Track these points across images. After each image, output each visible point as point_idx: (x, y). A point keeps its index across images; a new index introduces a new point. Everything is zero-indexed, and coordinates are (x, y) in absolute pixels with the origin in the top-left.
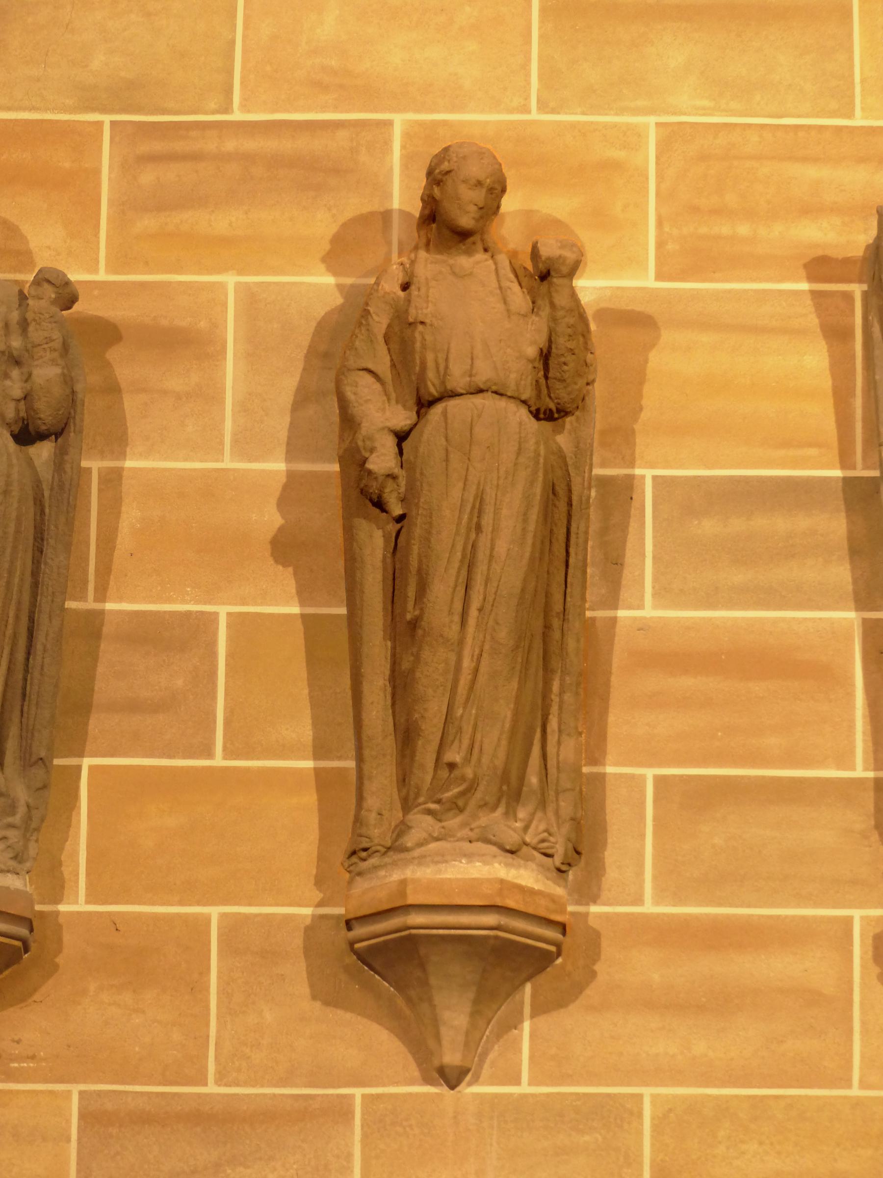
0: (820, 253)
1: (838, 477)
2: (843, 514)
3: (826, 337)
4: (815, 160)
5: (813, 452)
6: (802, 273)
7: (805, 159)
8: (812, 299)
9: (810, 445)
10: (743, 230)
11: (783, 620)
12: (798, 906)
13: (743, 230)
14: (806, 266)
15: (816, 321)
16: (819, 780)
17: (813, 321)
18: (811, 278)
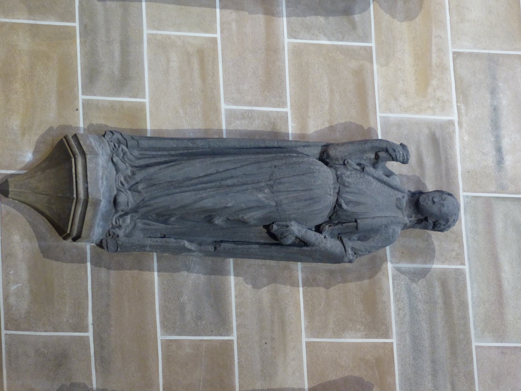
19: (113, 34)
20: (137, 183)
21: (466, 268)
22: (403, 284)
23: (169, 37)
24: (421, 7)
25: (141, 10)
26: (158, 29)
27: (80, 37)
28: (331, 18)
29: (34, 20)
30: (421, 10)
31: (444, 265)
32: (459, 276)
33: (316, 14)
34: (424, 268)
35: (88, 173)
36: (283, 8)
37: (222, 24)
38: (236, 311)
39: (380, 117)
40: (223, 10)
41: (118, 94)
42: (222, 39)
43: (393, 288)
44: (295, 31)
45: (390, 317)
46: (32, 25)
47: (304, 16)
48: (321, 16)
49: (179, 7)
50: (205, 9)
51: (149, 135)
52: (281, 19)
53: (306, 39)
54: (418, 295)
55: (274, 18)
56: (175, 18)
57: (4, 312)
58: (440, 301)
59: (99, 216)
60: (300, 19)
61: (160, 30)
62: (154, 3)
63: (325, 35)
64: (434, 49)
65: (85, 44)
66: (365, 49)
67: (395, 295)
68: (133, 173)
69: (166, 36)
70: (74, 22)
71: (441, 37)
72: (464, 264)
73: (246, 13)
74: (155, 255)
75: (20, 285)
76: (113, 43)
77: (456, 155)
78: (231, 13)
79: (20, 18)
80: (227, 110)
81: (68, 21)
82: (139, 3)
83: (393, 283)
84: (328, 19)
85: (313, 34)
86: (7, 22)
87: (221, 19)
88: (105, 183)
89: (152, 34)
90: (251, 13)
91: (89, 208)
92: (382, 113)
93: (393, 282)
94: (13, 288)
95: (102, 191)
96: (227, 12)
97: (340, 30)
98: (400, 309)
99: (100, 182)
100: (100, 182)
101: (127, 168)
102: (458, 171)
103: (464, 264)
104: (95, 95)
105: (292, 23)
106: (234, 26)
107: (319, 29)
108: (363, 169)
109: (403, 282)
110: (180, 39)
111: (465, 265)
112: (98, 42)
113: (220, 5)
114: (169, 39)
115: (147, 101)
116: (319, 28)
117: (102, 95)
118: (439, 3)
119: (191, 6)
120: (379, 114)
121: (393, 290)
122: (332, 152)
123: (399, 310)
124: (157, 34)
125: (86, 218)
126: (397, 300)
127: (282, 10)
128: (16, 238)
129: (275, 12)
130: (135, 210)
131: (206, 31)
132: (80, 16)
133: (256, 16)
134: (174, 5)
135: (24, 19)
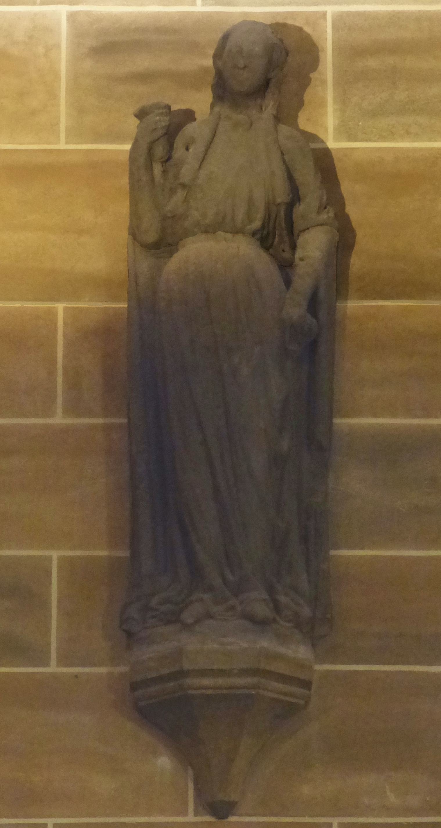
20: (225, 583)
21: (331, 10)
22: (362, 123)
31: (326, 48)
32: (345, 24)
34: (334, 85)
35: (215, 667)
38: (419, 417)
39: (67, 143)
41: (45, 604)
43: (370, 140)
45: (421, 149)
51: (124, 553)
54: (381, 98)
57: (435, 816)
58: (391, 60)
59: (282, 650)
67: (382, 138)
68: (211, 589)
72: (324, 14)
74: (333, 553)
75: (387, 787)
77: (131, 13)
80: (67, 412)
83: (363, 140)
88: (231, 640)
91: (272, 668)
92: (59, 140)
93: (360, 141)
94: (392, 799)
95: (245, 645)
98: (408, 133)
99: (229, 647)
100: (229, 647)
101: (201, 600)
102: (159, 12)
103: (324, 14)
104: (49, 644)
108: (184, 186)
109: (360, 123)
111: (326, 12)
115: (55, 555)
117: (48, 631)
120: (62, 146)
121: (375, 141)
122: (151, 237)
123: (408, 134)
125: (287, 672)
126: (391, 135)
128: (306, 790)
130: (271, 590)
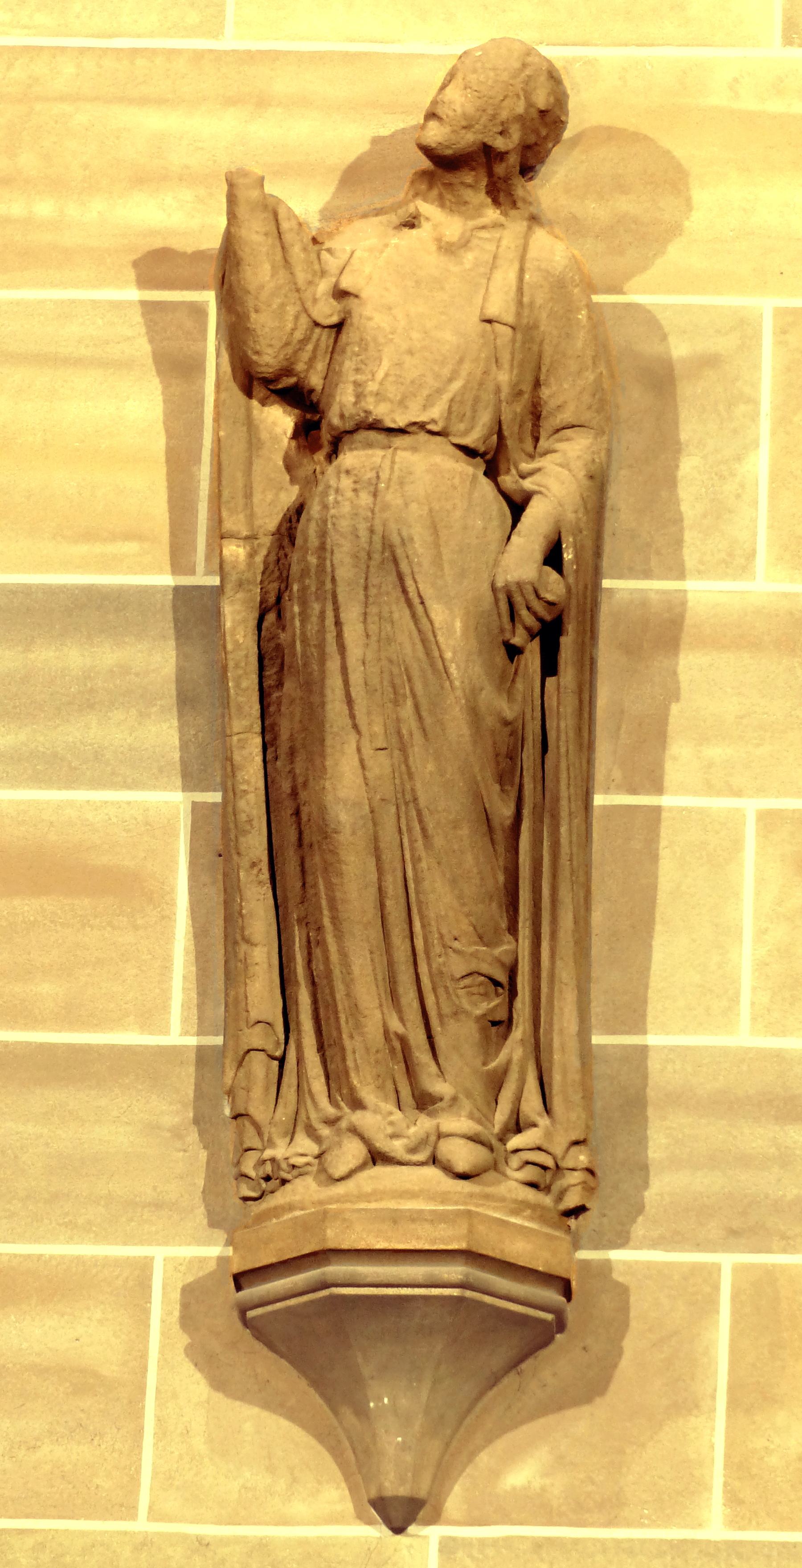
0: (158, 243)
1: (169, 586)
2: (172, 643)
3: (159, 372)
4: (161, 102)
5: (131, 547)
6: (131, 274)
7: (144, 101)
8: (143, 315)
9: (128, 537)
10: (44, 208)
11: (71, 804)
12: (70, 1240)
13: (44, 208)
14: (136, 264)
15: (147, 348)
16: (112, 1048)
17: (143, 348)
18: (144, 282)
19: (754, 1145)
23: (761, 965)
24: (636, 137)
25: (672, 1049)
26: (735, 1000)
27: (769, 1251)
28: (683, 436)
29: (713, 1397)
30: (646, 138)
33: (671, 482)
36: (651, 590)
37: (710, 789)
40: (667, 783)
42: (761, 791)
44: (730, 555)
46: (733, 1403)
47: (678, 520)
48: (677, 466)
49: (658, 927)
50: (663, 843)
52: (690, 596)
53: (754, 520)
55: (688, 622)
56: (694, 941)
60: (688, 536)
61: (737, 994)
62: (650, 1008)
63: (739, 459)
64: (775, 106)
65: (789, 1238)
66: (784, 332)
69: (757, 974)
70: (720, 1270)
71: (736, 80)
73: (675, 708)
76: (786, 1147)
78: (675, 759)
79: (711, 1440)
81: (716, 1288)
82: (651, 1054)
84: (687, 446)
85: (738, 496)
86: (726, 1484)
87: (696, 793)
89: (754, 1019)
90: (674, 695)
96: (672, 773)
97: (721, 407)
105: (701, 562)
106: (715, 752)
107: (721, 476)
110: (767, 930)
112: (784, 1195)
113: (648, 792)
114: (767, 965)
116: (716, 474)
118: (620, 78)
119: (654, 887)
124: (753, 1004)
127: (657, 592)
129: (666, 615)
131: (737, 844)
132: (699, 1246)
133: (684, 677)
134: (654, 943)
135: (713, 1429)
